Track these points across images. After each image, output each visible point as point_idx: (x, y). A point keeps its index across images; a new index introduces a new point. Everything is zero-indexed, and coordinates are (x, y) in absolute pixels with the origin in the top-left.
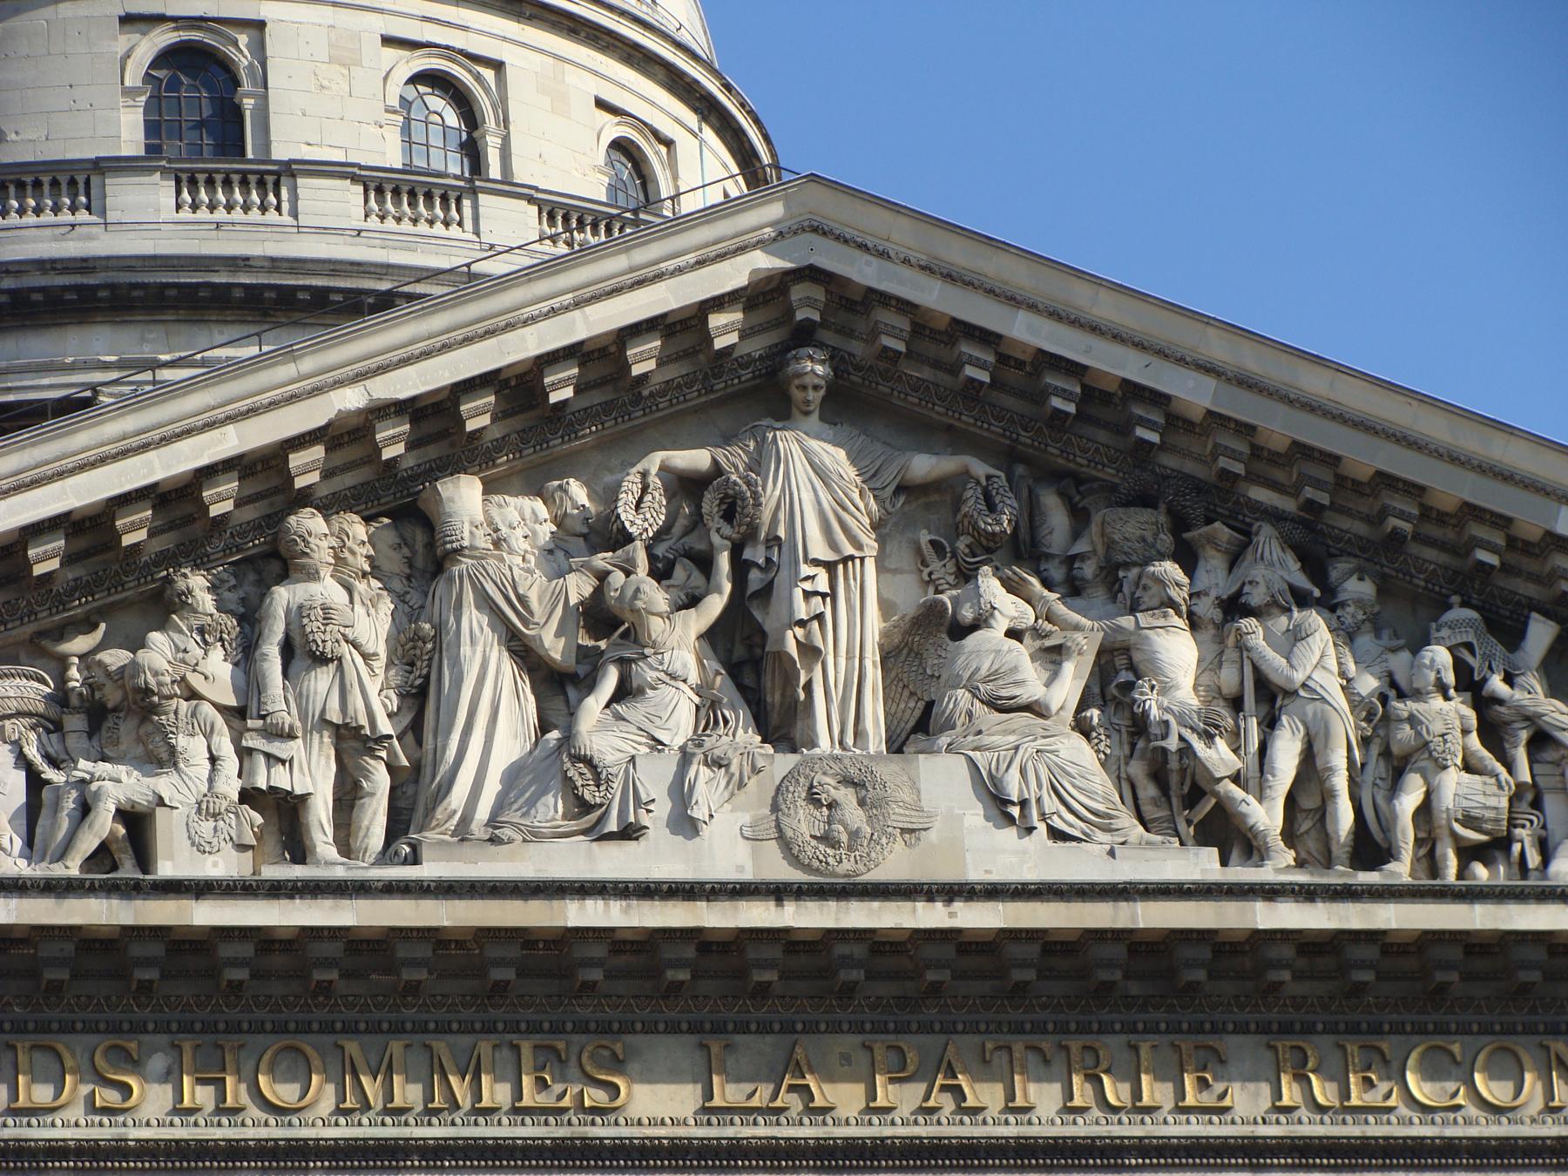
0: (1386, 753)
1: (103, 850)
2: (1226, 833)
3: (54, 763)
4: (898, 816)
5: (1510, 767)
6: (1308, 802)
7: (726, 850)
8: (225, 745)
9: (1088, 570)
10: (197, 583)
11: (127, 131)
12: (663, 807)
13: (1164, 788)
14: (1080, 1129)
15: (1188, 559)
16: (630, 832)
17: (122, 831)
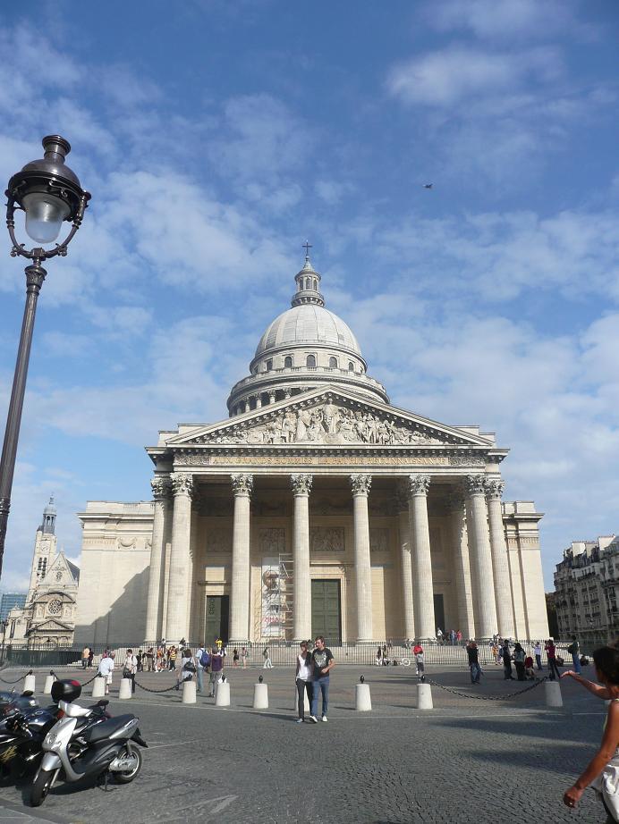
2: (365, 440)
7: (321, 442)
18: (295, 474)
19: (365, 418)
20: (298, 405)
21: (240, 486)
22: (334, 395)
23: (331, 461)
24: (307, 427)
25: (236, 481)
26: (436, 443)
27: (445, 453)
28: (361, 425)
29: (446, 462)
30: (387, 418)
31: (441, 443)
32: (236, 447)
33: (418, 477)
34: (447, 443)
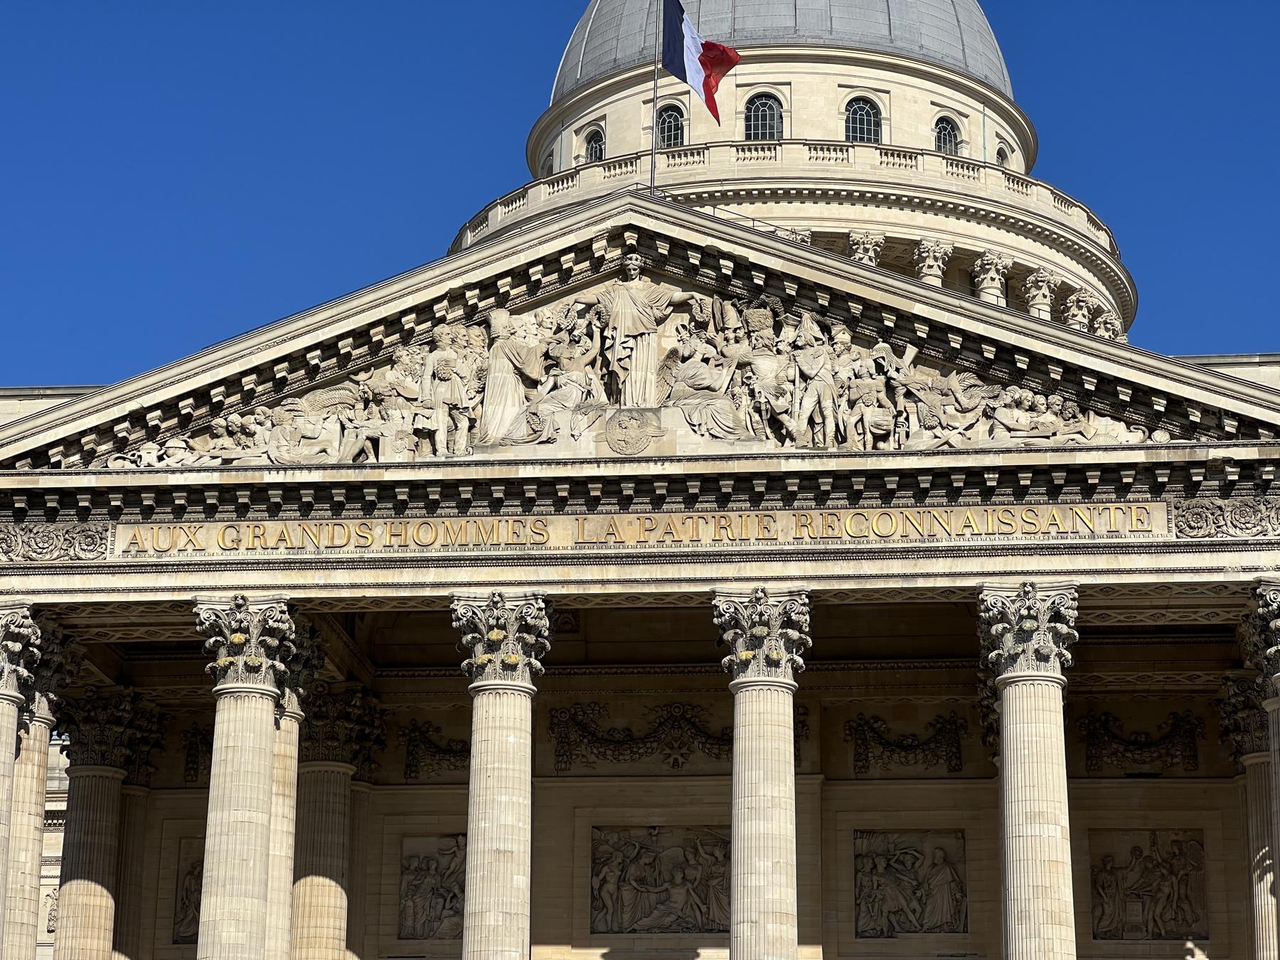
0: (849, 401)
1: (362, 451)
3: (351, 421)
4: (650, 430)
5: (895, 404)
6: (818, 419)
7: (587, 448)
8: (408, 415)
9: (741, 333)
10: (401, 352)
11: (646, 141)
12: (565, 431)
13: (761, 416)
14: (718, 548)
15: (778, 328)
16: (548, 441)
17: (369, 444)
18: (468, 590)
19: (788, 333)
20: (487, 287)
21: (236, 650)
22: (648, 238)
23: (631, 529)
24: (532, 383)
25: (216, 629)
26: (1109, 438)
27: (1150, 479)
28: (768, 368)
29: (1158, 521)
30: (886, 334)
31: (1136, 437)
32: (215, 478)
33: (1024, 593)
34: (1161, 437)
